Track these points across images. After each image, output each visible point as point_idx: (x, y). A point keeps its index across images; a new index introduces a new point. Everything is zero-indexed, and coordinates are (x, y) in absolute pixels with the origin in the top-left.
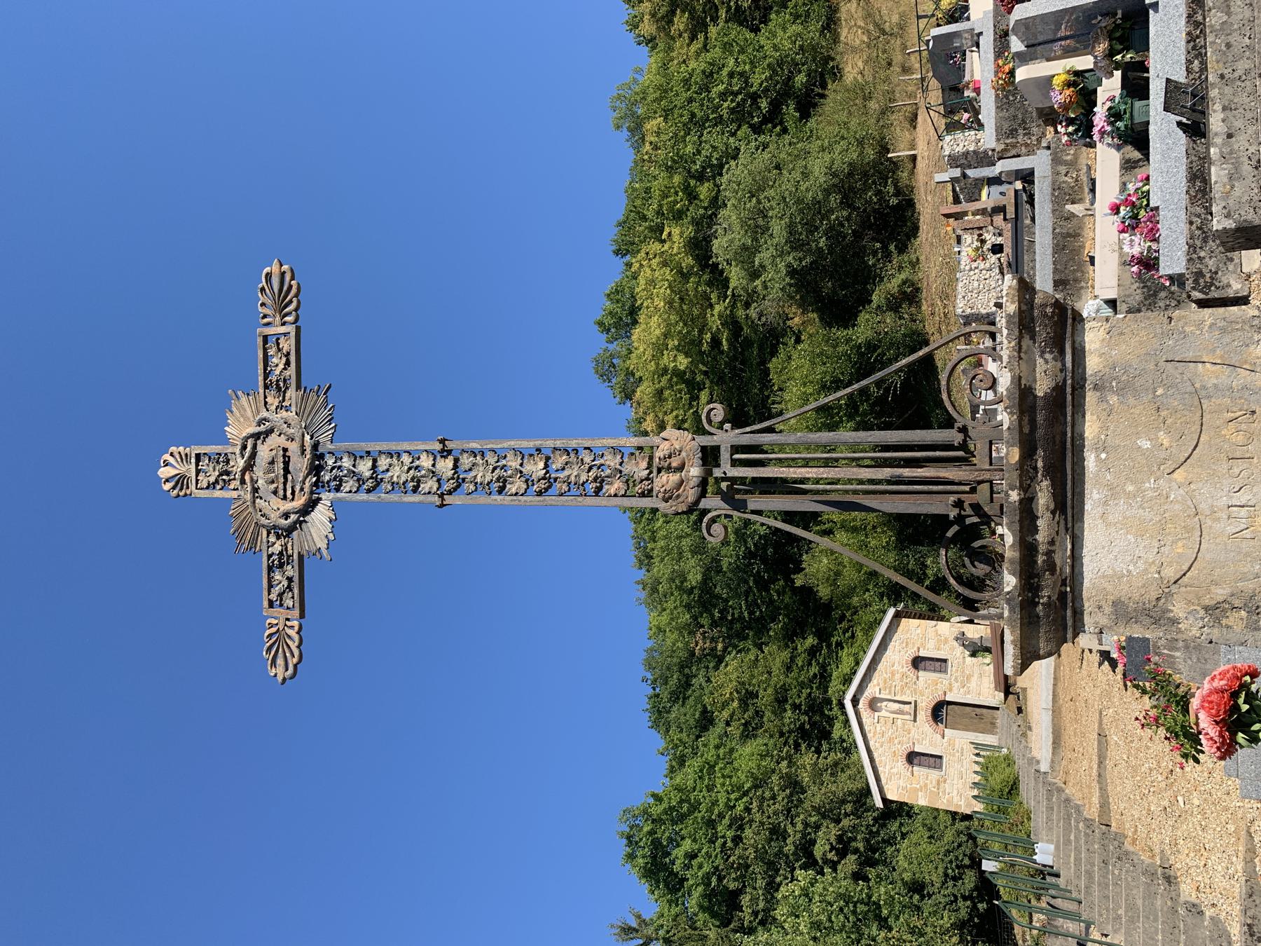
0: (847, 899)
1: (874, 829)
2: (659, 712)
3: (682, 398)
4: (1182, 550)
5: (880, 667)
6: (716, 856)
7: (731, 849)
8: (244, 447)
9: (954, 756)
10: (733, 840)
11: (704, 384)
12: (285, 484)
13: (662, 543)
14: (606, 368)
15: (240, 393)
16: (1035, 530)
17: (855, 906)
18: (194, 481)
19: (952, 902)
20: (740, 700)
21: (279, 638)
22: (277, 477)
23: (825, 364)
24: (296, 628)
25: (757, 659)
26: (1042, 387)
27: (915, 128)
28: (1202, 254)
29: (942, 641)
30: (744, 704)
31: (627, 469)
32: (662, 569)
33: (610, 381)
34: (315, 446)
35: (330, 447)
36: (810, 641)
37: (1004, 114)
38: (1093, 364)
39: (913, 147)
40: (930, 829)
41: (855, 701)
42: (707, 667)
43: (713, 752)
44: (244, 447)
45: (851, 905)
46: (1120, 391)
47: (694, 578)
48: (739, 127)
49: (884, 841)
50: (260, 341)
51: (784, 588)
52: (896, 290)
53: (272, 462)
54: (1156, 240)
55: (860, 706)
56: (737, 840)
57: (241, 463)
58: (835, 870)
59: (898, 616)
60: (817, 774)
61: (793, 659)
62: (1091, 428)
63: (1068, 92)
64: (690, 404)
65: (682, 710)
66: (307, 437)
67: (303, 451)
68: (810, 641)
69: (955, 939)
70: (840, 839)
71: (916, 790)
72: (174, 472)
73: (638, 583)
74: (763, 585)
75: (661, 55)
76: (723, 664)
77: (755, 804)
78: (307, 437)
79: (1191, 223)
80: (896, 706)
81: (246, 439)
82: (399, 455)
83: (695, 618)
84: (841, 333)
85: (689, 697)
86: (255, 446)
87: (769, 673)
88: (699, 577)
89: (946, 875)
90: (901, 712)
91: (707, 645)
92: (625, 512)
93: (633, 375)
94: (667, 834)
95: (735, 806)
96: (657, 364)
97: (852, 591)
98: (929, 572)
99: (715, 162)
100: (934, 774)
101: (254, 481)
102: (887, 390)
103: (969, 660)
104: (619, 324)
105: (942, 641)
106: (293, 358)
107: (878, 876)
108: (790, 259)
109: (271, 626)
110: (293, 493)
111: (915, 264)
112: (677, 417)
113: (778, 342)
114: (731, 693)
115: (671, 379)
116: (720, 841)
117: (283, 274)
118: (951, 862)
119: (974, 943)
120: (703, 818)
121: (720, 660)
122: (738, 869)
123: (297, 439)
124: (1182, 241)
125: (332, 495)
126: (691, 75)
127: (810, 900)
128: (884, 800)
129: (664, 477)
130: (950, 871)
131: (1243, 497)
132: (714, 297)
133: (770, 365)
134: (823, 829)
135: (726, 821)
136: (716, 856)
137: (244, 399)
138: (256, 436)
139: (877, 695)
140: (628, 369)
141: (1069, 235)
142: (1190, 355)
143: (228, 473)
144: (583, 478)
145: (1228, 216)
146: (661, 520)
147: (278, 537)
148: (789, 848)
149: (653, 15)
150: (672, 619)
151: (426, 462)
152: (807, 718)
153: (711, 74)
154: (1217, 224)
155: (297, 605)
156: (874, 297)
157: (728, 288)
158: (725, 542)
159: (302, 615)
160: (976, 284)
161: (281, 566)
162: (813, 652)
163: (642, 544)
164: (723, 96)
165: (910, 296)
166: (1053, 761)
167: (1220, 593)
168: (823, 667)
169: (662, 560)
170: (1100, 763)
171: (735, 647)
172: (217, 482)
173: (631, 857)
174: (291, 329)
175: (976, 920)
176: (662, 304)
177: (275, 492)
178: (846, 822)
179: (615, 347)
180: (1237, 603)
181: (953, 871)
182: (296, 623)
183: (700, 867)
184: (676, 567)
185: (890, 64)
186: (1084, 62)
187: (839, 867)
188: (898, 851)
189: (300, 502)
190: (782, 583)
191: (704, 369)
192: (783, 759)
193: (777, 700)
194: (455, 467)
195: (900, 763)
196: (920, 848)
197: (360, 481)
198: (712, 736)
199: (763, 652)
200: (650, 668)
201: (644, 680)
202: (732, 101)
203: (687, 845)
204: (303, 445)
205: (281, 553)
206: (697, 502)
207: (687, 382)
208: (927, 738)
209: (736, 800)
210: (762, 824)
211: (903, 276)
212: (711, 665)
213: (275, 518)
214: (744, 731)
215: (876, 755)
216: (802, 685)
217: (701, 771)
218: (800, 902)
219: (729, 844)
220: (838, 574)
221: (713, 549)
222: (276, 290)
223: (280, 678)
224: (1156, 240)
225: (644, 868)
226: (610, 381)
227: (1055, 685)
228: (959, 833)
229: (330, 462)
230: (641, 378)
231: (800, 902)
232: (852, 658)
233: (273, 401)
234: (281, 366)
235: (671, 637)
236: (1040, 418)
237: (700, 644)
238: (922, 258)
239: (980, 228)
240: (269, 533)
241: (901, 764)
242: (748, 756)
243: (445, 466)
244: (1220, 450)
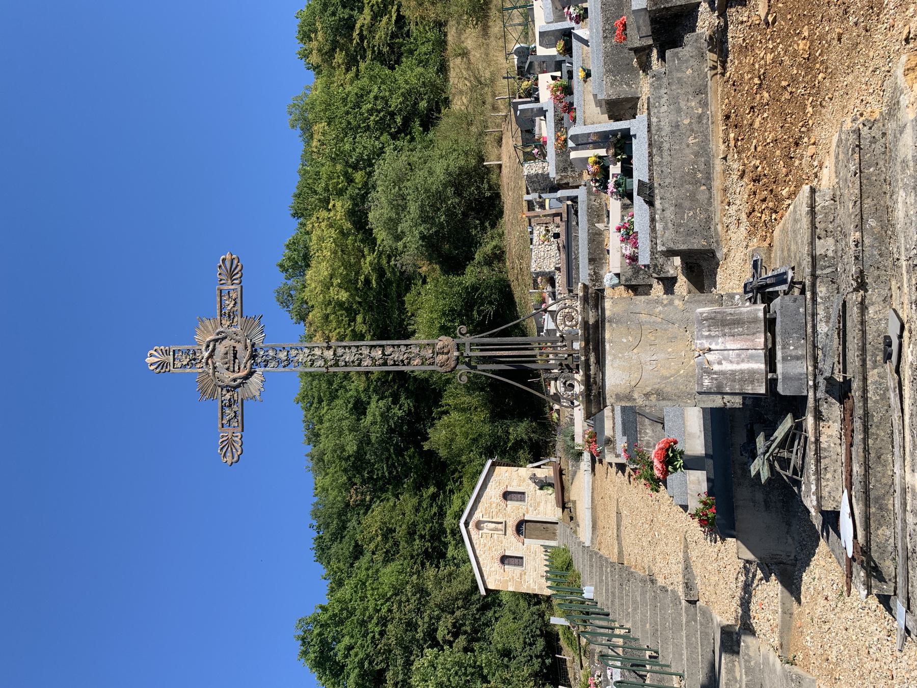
0: (459, 664)
1: (477, 616)
2: (323, 550)
4: (637, 375)
5: (483, 499)
6: (368, 646)
7: (379, 640)
8: (208, 346)
9: (530, 556)
10: (379, 634)
11: (359, 311)
12: (234, 364)
13: (328, 424)
14: (285, 299)
15: (204, 319)
16: (590, 370)
17: (466, 669)
18: (172, 365)
19: (529, 661)
20: (382, 535)
21: (230, 443)
22: (229, 361)
23: (444, 299)
24: (240, 437)
25: (395, 505)
26: (591, 321)
27: (501, 146)
28: (657, 256)
29: (521, 480)
30: (385, 537)
31: (422, 353)
32: (327, 443)
33: (288, 307)
34: (253, 345)
35: (261, 345)
36: (432, 490)
37: (560, 158)
38: (608, 313)
39: (499, 159)
40: (514, 613)
41: (467, 524)
42: (358, 514)
43: (364, 573)
44: (208, 346)
45: (463, 669)
46: (616, 323)
47: (351, 448)
48: (382, 134)
49: (484, 624)
50: (218, 292)
51: (414, 453)
52: (490, 252)
53: (226, 354)
54: (637, 248)
55: (470, 527)
56: (382, 634)
57: (206, 354)
58: (451, 647)
59: (494, 465)
60: (438, 582)
61: (420, 503)
62: (607, 335)
63: (596, 167)
65: (340, 546)
66: (248, 341)
67: (246, 348)
68: (432, 490)
69: (532, 684)
70: (454, 625)
71: (507, 581)
72: (156, 360)
73: (307, 455)
74: (400, 452)
75: (325, 78)
76: (370, 510)
77: (395, 606)
78: (248, 341)
79: (652, 241)
80: (493, 525)
81: (209, 342)
82: (302, 349)
83: (349, 479)
84: (455, 279)
86: (215, 346)
87: (404, 514)
88: (355, 448)
89: (525, 643)
90: (496, 529)
91: (359, 497)
92: (298, 403)
93: (307, 303)
94: (331, 634)
95: (381, 609)
96: (324, 297)
97: (461, 452)
98: (511, 437)
99: (366, 157)
100: (518, 569)
101: (214, 364)
102: (485, 317)
103: (538, 492)
104: (295, 265)
105: (521, 480)
106: (239, 301)
107: (480, 648)
108: (422, 228)
109: (223, 437)
110: (239, 369)
111: (501, 235)
112: (339, 333)
113: (411, 283)
114: (376, 531)
115: (335, 307)
116: (371, 635)
117: (232, 260)
118: (528, 634)
119: (544, 685)
120: (358, 619)
121: (368, 508)
122: (384, 653)
123: (243, 342)
124: (648, 249)
125: (263, 369)
126: (348, 96)
127: (435, 668)
128: (486, 589)
129: (440, 357)
130: (527, 640)
131: (654, 358)
133: (405, 299)
134: (443, 619)
135: (375, 620)
136: (368, 646)
137: (207, 322)
138: (216, 340)
139: (481, 519)
140: (302, 299)
141: (596, 234)
142: (637, 311)
143: (194, 359)
144: (401, 358)
145: (663, 245)
146: (326, 408)
147: (228, 391)
148: (419, 635)
149: (319, 51)
150: (333, 480)
152: (430, 544)
153: (362, 96)
154: (660, 248)
155: (240, 425)
156: (476, 256)
158: (374, 423)
159: (243, 431)
160: (542, 253)
161: (230, 406)
162: (434, 497)
163: (311, 426)
164: (371, 112)
165: (498, 256)
166: (592, 538)
167: (648, 389)
168: (441, 508)
169: (327, 437)
170: (618, 529)
171: (379, 498)
172: (188, 364)
173: (305, 653)
174: (238, 287)
175: (545, 671)
176: (329, 254)
177: (228, 369)
178: (458, 613)
179: (291, 282)
180: (653, 392)
181: (530, 639)
182: (239, 434)
183: (356, 655)
184: (338, 442)
185: (484, 103)
186: (602, 152)
187: (454, 645)
188: (493, 630)
189: (243, 373)
190: (412, 450)
191: (360, 300)
192: (414, 574)
193: (409, 533)
194: (335, 354)
195: (496, 564)
196: (508, 626)
197: (279, 362)
198: (364, 561)
199: (399, 500)
200: (316, 516)
201: (311, 526)
202: (377, 116)
203: (346, 641)
204: (246, 345)
205: (230, 399)
206: (455, 367)
207: (347, 310)
208: (513, 545)
209: (382, 605)
210: (400, 619)
211: (494, 243)
212: (362, 512)
213: (227, 381)
214: (385, 557)
215: (480, 559)
216: (426, 521)
217: (356, 587)
218: (428, 671)
219: (377, 636)
220: (452, 440)
221: (364, 427)
223: (229, 463)
224: (637, 248)
225: (315, 660)
226: (288, 307)
228: (533, 614)
229: (262, 353)
230: (313, 306)
231: (428, 671)
232: (460, 500)
233: (226, 322)
234: (231, 305)
235: (333, 494)
236: (591, 332)
237: (354, 498)
238: (506, 232)
239: (547, 224)
240: (222, 389)
241: (497, 565)
242: (389, 574)
243: (329, 354)
244: (647, 342)
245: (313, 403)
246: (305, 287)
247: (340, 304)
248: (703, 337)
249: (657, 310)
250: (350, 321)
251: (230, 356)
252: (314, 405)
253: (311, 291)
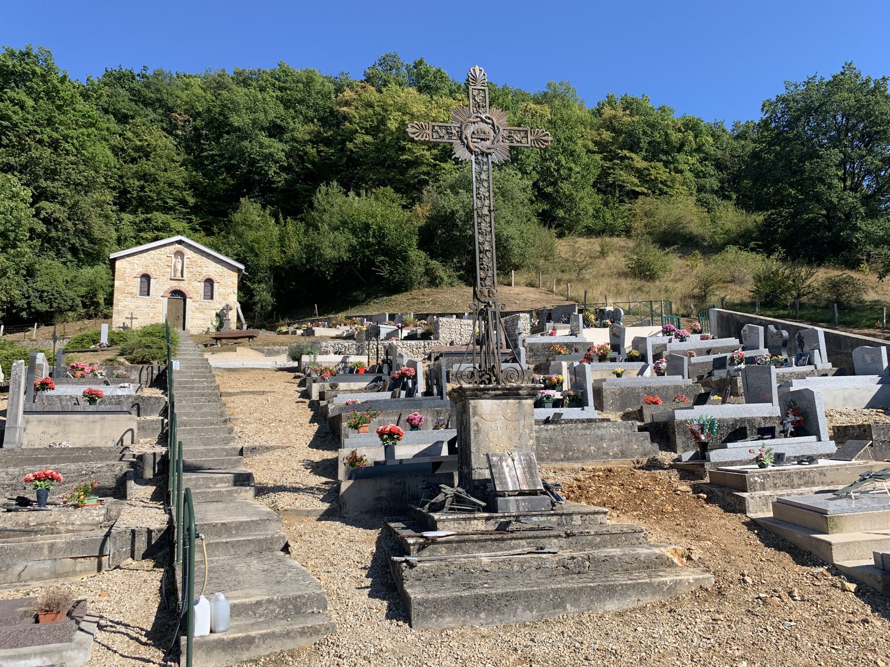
0: (19, 224)
1: (67, 244)
2: (121, 78)
3: (367, 122)
4: (488, 418)
5: (205, 259)
6: (26, 126)
7: (35, 138)
9: (151, 303)
10: (39, 139)
11: (376, 139)
13: (260, 97)
14: (388, 63)
17: (12, 231)
18: (475, 87)
19: (23, 295)
20: (142, 146)
23: (396, 230)
25: (174, 161)
26: (521, 392)
27: (526, 286)
29: (225, 296)
30: (137, 149)
32: (240, 94)
33: (380, 65)
34: (490, 154)
36: (191, 201)
37: (540, 347)
38: (524, 401)
39: (516, 284)
40: (72, 281)
41: (180, 242)
42: (162, 121)
43: (105, 126)
44: (489, 119)
45: (13, 228)
47: (236, 120)
48: (538, 172)
49: (59, 250)
51: (228, 184)
52: (438, 274)
55: (177, 246)
56: (40, 142)
57: (483, 117)
58: (34, 216)
59: (239, 270)
60: (100, 204)
61: (177, 188)
62: (511, 401)
63: (556, 380)
64: (363, 128)
65: (126, 99)
67: (489, 149)
68: (191, 201)
69: (4, 299)
70: (56, 220)
71: (124, 280)
72: (477, 75)
73: (223, 70)
74: (229, 169)
75: (589, 120)
76: (167, 135)
77: (73, 158)
80: (179, 268)
81: (492, 120)
83: (199, 114)
84: (415, 241)
85: (137, 104)
87: (165, 170)
88: (236, 124)
89: (43, 292)
90: (175, 271)
91: (180, 123)
92: (279, 65)
93: (385, 85)
94: (36, 86)
95: (69, 143)
96: (391, 105)
97: (240, 236)
98: (256, 286)
99: (519, 157)
100: (137, 290)
102: (378, 267)
103: (214, 312)
104: (420, 76)
105: (225, 296)
107: (35, 246)
108: (461, 212)
111: (451, 285)
112: (354, 117)
113: (403, 193)
114: (146, 140)
115: (380, 114)
116: (38, 130)
118: (53, 295)
119: (3, 310)
120: (55, 117)
121: (170, 133)
122: (20, 143)
126: (574, 142)
127: (10, 198)
128: (115, 259)
130: (46, 294)
132: (435, 152)
133: (389, 188)
134: (62, 208)
135: (55, 135)
136: (26, 126)
138: (493, 125)
139: (185, 257)
140: (389, 82)
146: (274, 94)
148: (43, 183)
149: (615, 117)
150: (197, 97)
151: (487, 202)
152: (135, 196)
153: (572, 155)
156: (434, 262)
157: (441, 162)
158: (261, 146)
160: (454, 327)
161: (448, 133)
162: (183, 202)
163: (254, 76)
164: (558, 163)
165: (434, 281)
166: (220, 368)
167: (480, 425)
168: (172, 209)
169: (247, 95)
170: (250, 392)
171: (179, 143)
173: (12, 54)
175: (14, 311)
176: (434, 115)
177: (473, 133)
178: (69, 224)
179: (404, 71)
181: (46, 297)
183: (14, 112)
184: (242, 106)
185: (563, 271)
186: (566, 387)
187: (35, 219)
188: (53, 259)
190: (232, 182)
191: (387, 141)
192: (105, 179)
193: (145, 175)
195: (141, 270)
196: (59, 275)
198: (114, 126)
199: (180, 167)
200: (156, 75)
201: (145, 68)
202: (554, 169)
203: (30, 103)
205: (452, 133)
207: (378, 127)
208: (161, 287)
209: (73, 144)
210: (59, 164)
211: (445, 278)
212: (164, 125)
214: (118, 148)
215: (145, 254)
216: (159, 194)
217: (89, 117)
218: (8, 192)
219: (38, 137)
220: (250, 227)
221: (257, 135)
222: (543, 138)
225: (4, 66)
226: (380, 65)
227: (260, 369)
228: (73, 300)
230: (381, 92)
231: (8, 192)
232: (181, 229)
234: (517, 139)
235: (184, 95)
237: (179, 117)
238: (454, 289)
241: (141, 270)
242: (103, 152)
245: (279, 81)
246: (400, 85)
247: (383, 121)
248: (520, 456)
249: (527, 430)
250: (366, 129)
251: (482, 136)
252: (277, 83)
253: (396, 91)
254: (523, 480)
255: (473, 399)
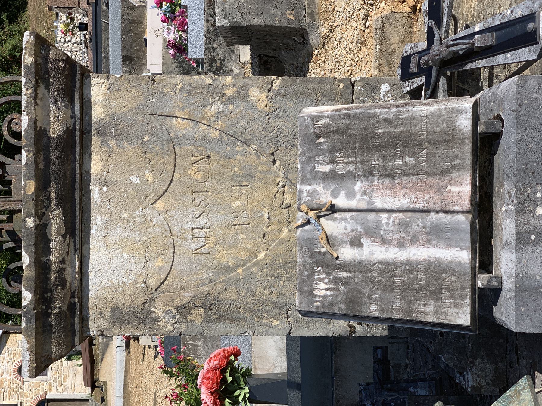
16: (49, 251)
28: (215, 45)
46: (118, 137)
52: (7, 53)
54: (185, 31)
79: (208, 21)
124: (202, 34)
131: (202, 222)
141: (133, 22)
142: (167, 111)
145: (225, 17)
154: (220, 22)
167: (187, 295)
180: (198, 302)
224: (185, 31)
227: (125, 376)
236: (53, 156)
239: (70, 8)
244: (186, 185)
248: (316, 176)
249: (212, 110)
254: (424, 188)
255: (84, 320)
